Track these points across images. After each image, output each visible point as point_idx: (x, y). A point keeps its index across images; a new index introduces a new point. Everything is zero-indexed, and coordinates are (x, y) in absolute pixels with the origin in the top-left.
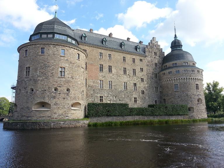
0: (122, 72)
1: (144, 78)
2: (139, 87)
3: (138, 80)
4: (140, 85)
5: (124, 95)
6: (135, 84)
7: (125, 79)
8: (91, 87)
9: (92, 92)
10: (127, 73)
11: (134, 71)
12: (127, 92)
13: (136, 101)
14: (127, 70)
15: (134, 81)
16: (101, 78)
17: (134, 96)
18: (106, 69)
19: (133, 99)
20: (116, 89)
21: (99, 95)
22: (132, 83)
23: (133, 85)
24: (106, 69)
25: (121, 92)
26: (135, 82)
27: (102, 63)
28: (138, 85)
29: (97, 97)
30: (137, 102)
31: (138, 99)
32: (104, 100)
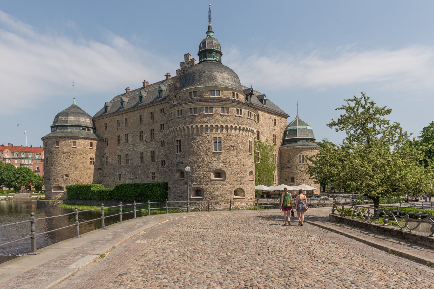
0: (138, 139)
1: (165, 140)
2: (159, 156)
3: (156, 146)
4: (159, 152)
5: (141, 169)
6: (153, 153)
7: (142, 148)
8: (112, 165)
9: (113, 171)
10: (144, 139)
11: (152, 131)
12: (144, 167)
13: (153, 177)
14: (144, 133)
15: (152, 147)
16: (119, 153)
17: (152, 170)
18: (123, 140)
19: (151, 175)
20: (132, 164)
21: (117, 174)
22: (149, 150)
23: (149, 154)
24: (123, 140)
25: (138, 166)
26: (153, 150)
27: (119, 133)
28: (157, 153)
29: (116, 175)
30: (156, 179)
31: (156, 174)
32: (122, 178)
